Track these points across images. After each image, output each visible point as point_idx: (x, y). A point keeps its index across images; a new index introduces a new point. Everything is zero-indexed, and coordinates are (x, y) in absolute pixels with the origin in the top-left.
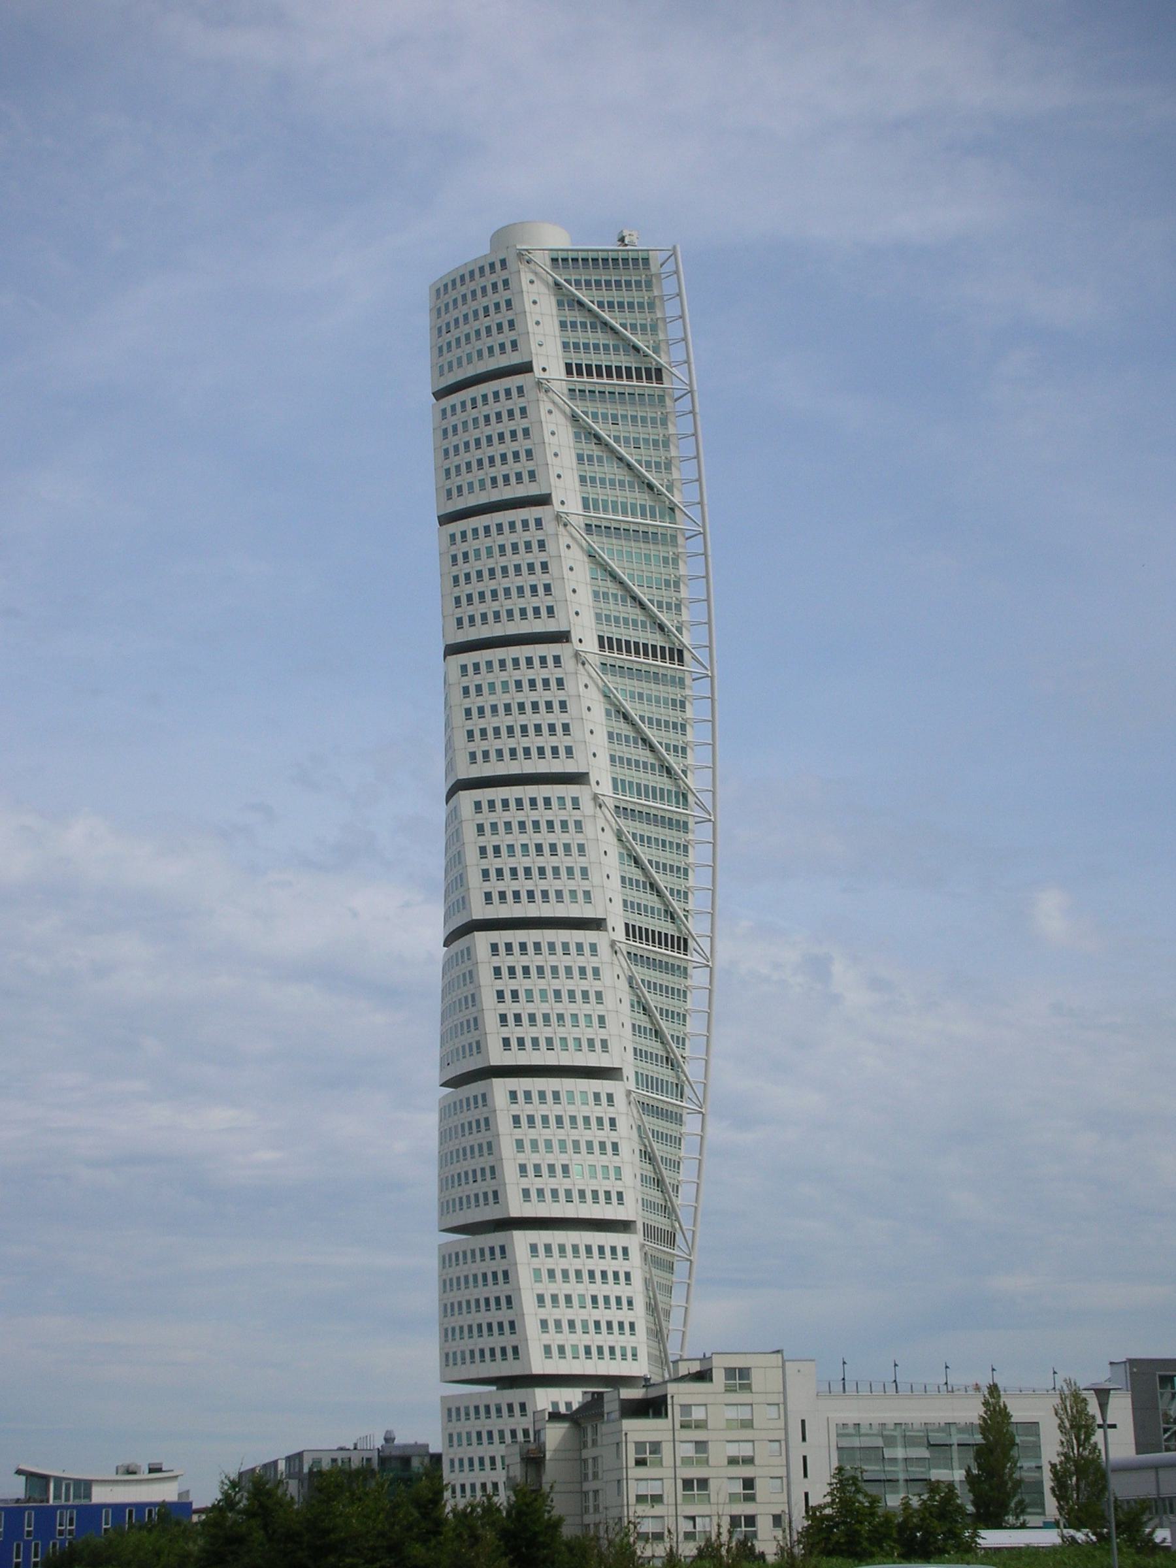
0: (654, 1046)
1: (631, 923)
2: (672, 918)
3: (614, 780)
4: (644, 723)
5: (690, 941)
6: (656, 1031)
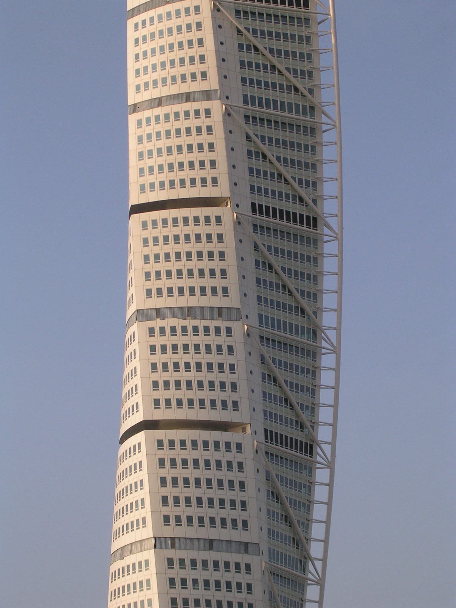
0: (283, 528)
1: (269, 429)
2: (302, 427)
3: (260, 316)
4: (285, 273)
5: (315, 445)
6: (286, 517)
